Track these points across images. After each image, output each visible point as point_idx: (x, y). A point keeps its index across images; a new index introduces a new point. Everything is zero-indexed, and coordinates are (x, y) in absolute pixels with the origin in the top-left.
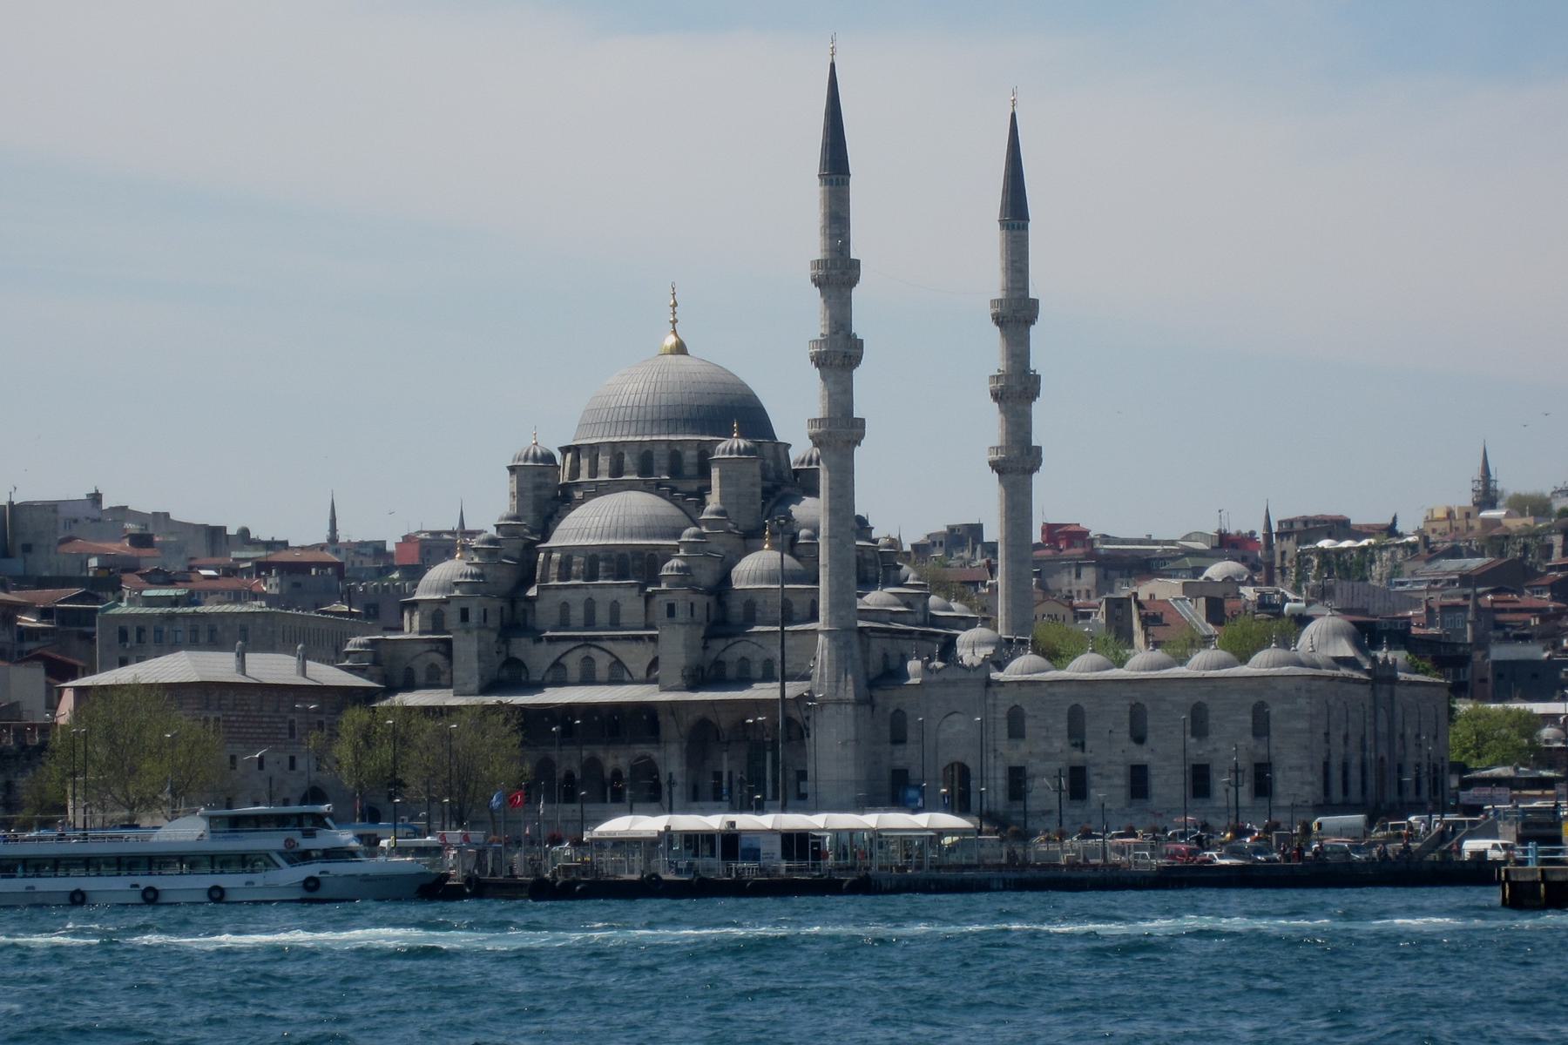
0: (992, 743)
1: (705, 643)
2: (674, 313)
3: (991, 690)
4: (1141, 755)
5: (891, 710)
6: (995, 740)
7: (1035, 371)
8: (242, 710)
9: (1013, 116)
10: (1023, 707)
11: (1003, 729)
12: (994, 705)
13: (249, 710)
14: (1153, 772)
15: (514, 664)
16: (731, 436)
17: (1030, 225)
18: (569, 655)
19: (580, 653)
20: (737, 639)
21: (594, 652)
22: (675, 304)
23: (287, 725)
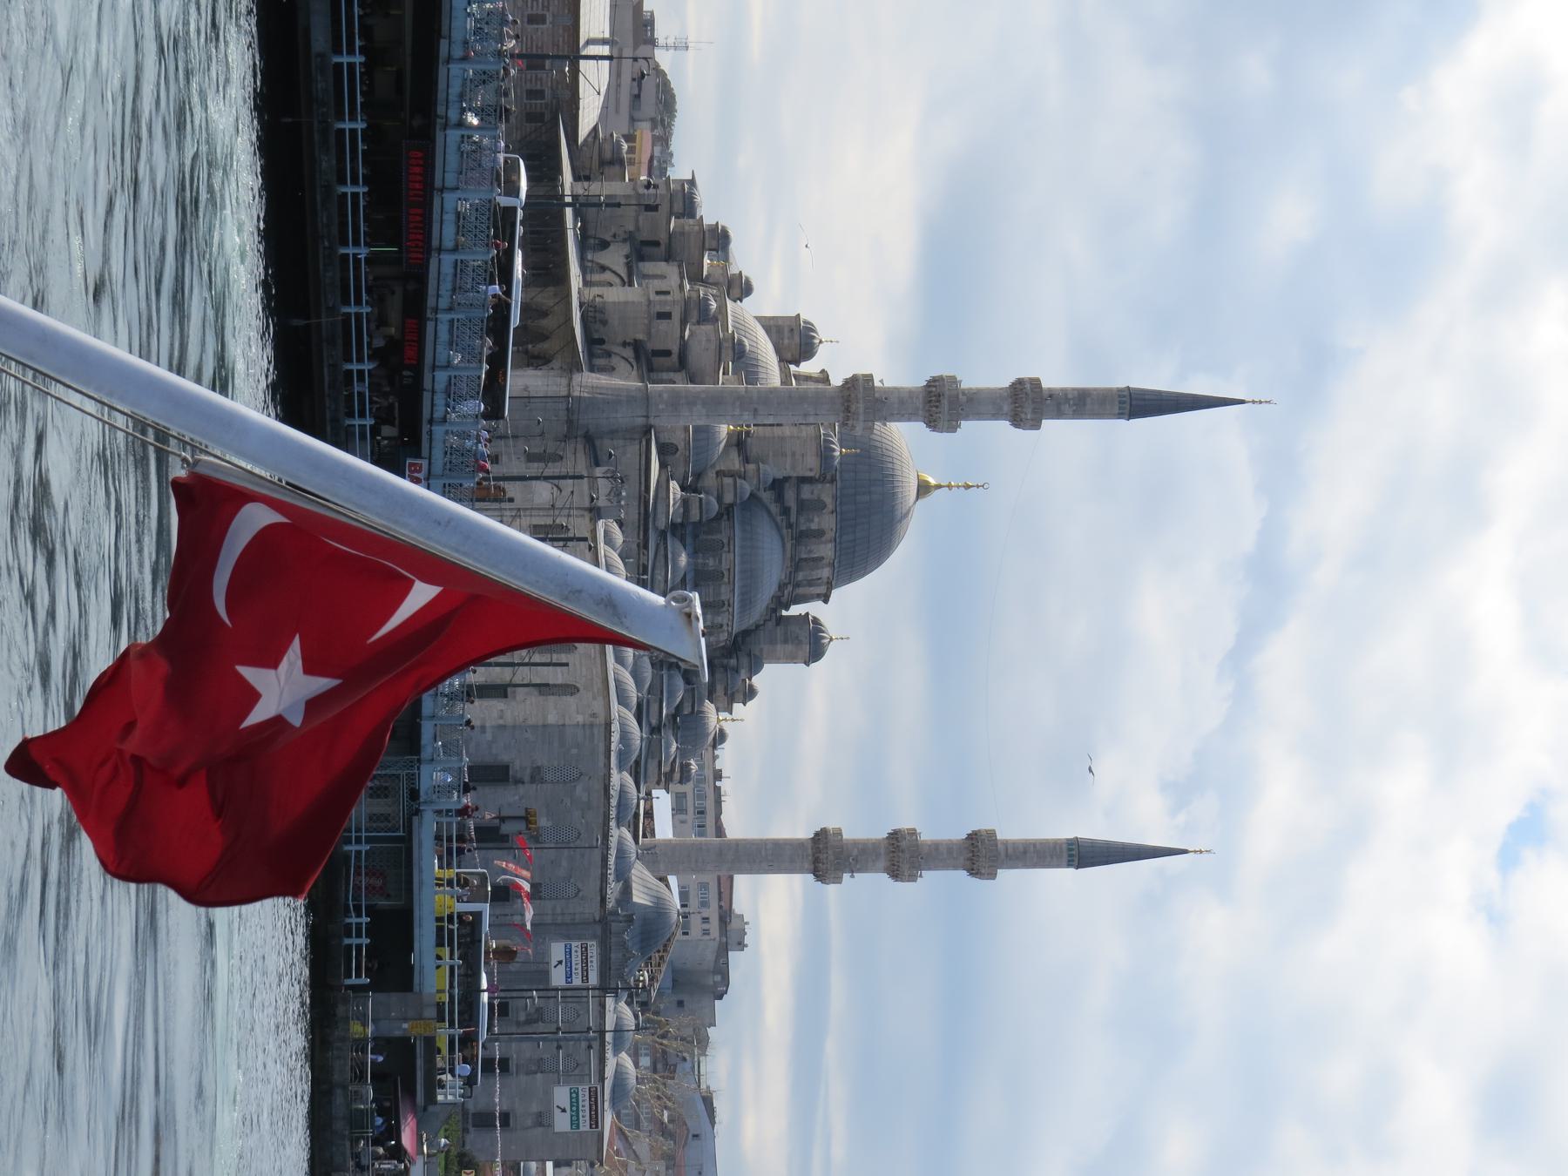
1: (629, 344)
2: (958, 487)
7: (921, 876)
9: (1185, 852)
15: (604, 245)
16: (841, 448)
17: (1072, 870)
19: (617, 280)
22: (967, 487)
23: (540, 12)
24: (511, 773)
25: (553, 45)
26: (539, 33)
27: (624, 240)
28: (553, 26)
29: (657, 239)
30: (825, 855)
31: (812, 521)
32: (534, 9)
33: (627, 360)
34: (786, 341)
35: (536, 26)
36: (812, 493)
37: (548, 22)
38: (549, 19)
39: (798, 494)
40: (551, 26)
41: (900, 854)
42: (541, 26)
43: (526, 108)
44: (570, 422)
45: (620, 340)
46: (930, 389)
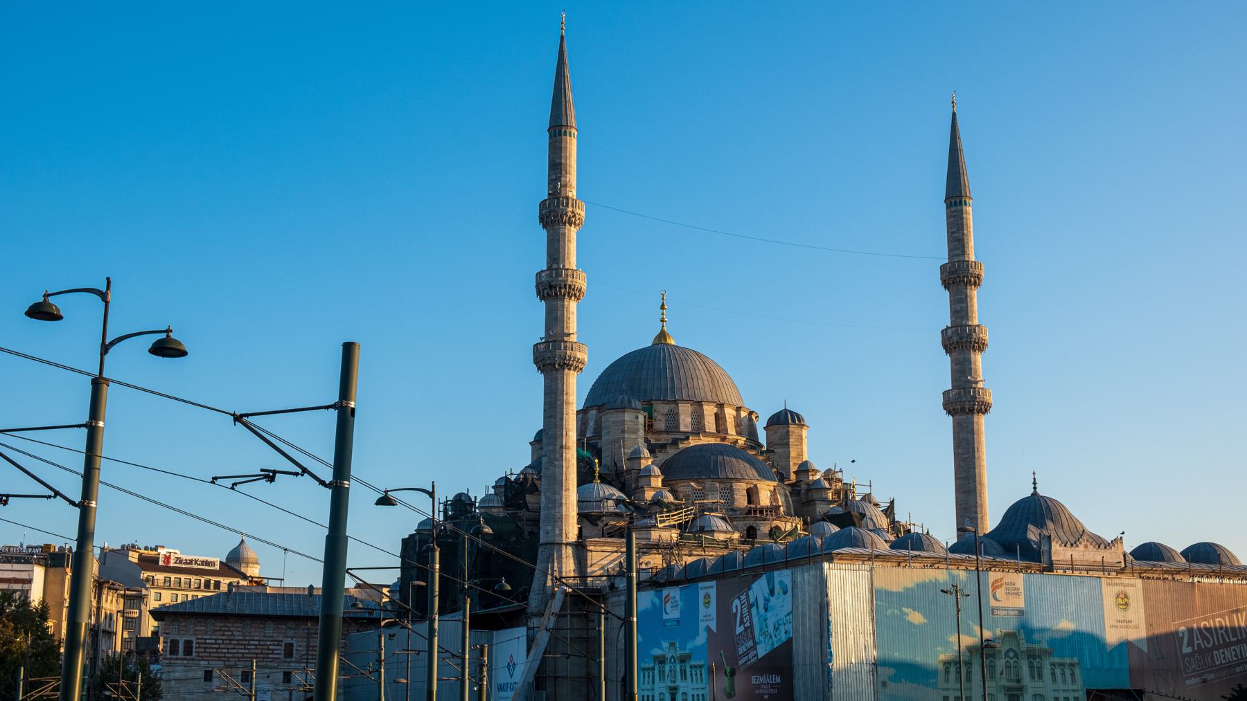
2: (663, 314)
8: (224, 635)
9: (954, 114)
13: (232, 635)
23: (283, 648)
26: (300, 648)
28: (295, 637)
30: (967, 403)
32: (279, 652)
35: (294, 651)
36: (660, 421)
37: (292, 642)
38: (289, 640)
39: (661, 432)
40: (294, 639)
41: (964, 340)
42: (295, 647)
46: (546, 295)
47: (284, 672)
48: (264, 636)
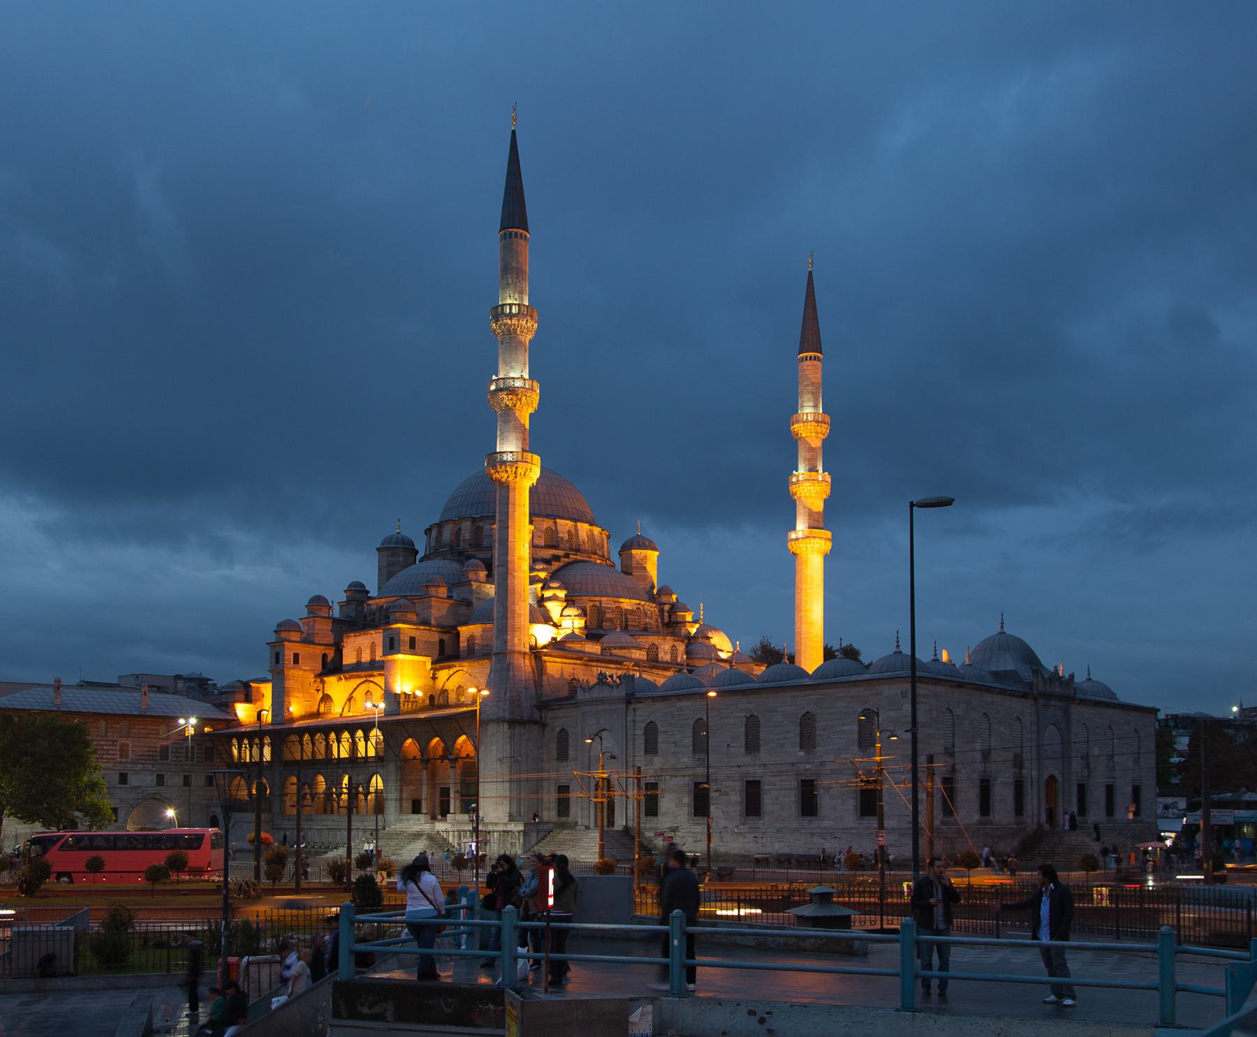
0: (631, 759)
1: (434, 675)
3: (632, 706)
4: (757, 772)
5: (558, 730)
6: (634, 756)
10: (657, 723)
11: (640, 743)
12: (634, 721)
14: (765, 787)
15: (326, 698)
18: (357, 690)
19: (364, 688)
20: (455, 669)
21: (371, 684)
23: (118, 748)
24: (948, 776)
25: (147, 737)
26: (137, 749)
27: (323, 682)
29: (321, 656)
31: (562, 538)
33: (450, 677)
34: (401, 559)
38: (124, 741)
39: (541, 547)
43: (201, 762)
44: (531, 722)
45: (430, 682)
47: (120, 773)
48: (98, 736)
